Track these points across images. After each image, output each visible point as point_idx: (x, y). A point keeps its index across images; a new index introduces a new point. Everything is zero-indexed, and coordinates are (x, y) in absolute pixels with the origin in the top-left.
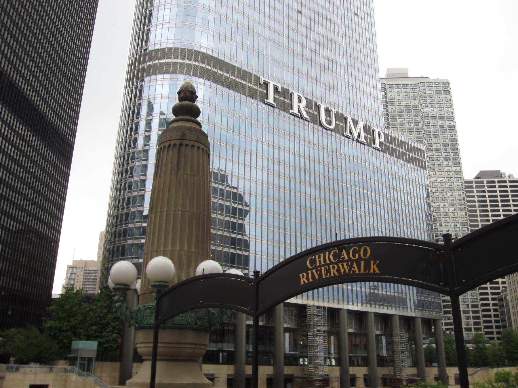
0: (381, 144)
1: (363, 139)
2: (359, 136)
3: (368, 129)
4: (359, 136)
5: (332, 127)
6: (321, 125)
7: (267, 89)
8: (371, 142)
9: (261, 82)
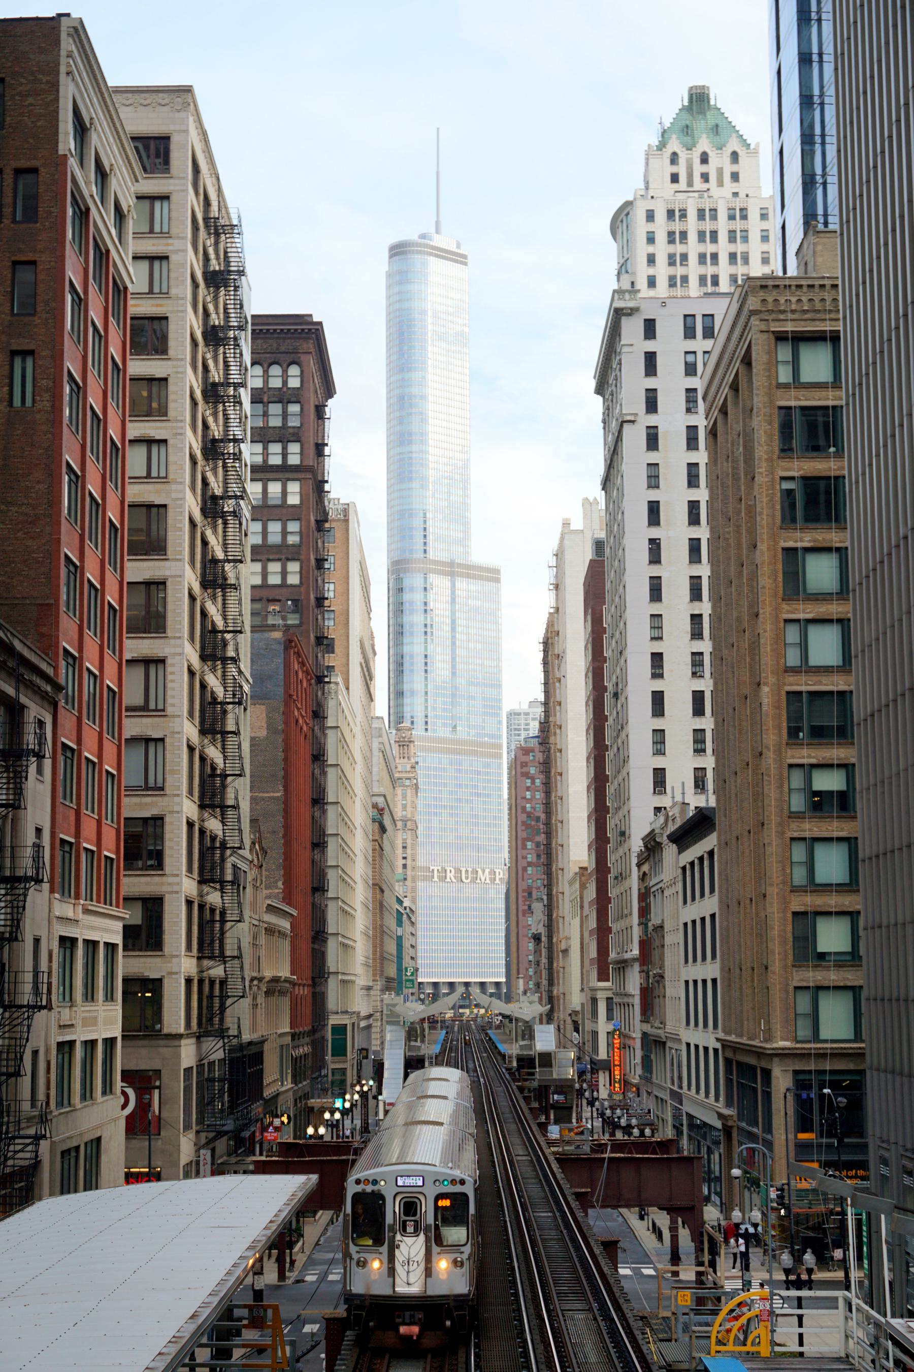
1: (488, 881)
5: (469, 881)
6: (462, 881)
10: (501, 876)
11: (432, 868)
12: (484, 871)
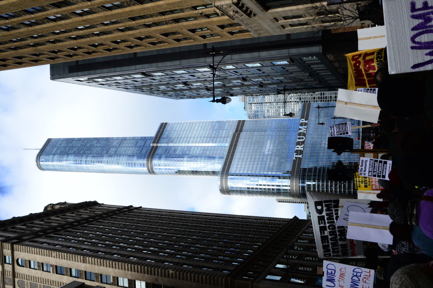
0: (306, 120)
1: (306, 127)
2: (305, 128)
3: (302, 124)
4: (305, 128)
5: (304, 137)
6: (304, 141)
7: (297, 157)
8: (306, 124)
9: (295, 159)
10: (304, 120)
11: (294, 159)
12: (300, 129)
